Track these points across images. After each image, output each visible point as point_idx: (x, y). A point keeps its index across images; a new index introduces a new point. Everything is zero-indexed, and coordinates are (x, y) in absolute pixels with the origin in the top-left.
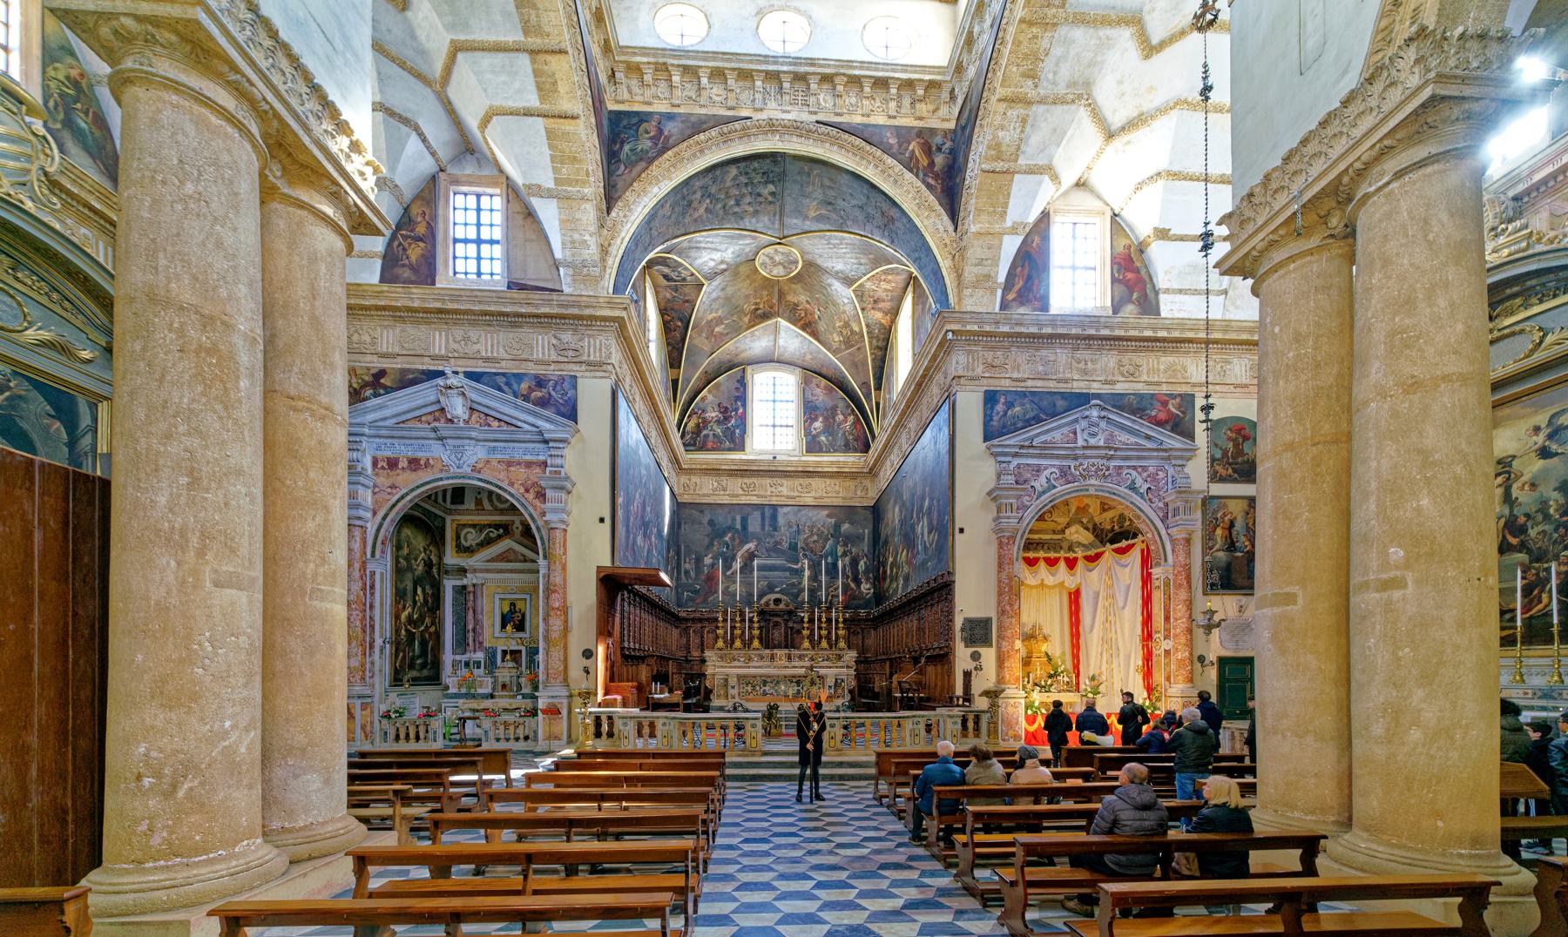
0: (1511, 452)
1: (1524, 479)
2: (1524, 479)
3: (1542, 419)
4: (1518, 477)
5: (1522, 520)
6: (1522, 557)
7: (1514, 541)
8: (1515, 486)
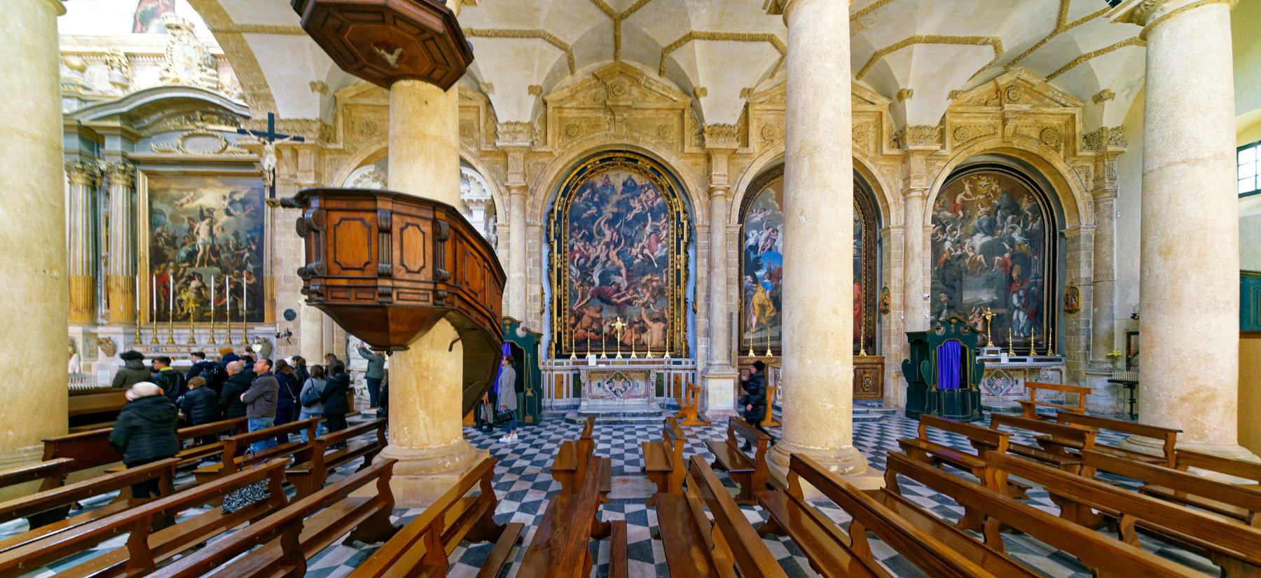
2: (219, 224)
3: (227, 192)
4: (215, 223)
5: (218, 248)
6: (217, 269)
7: (214, 259)
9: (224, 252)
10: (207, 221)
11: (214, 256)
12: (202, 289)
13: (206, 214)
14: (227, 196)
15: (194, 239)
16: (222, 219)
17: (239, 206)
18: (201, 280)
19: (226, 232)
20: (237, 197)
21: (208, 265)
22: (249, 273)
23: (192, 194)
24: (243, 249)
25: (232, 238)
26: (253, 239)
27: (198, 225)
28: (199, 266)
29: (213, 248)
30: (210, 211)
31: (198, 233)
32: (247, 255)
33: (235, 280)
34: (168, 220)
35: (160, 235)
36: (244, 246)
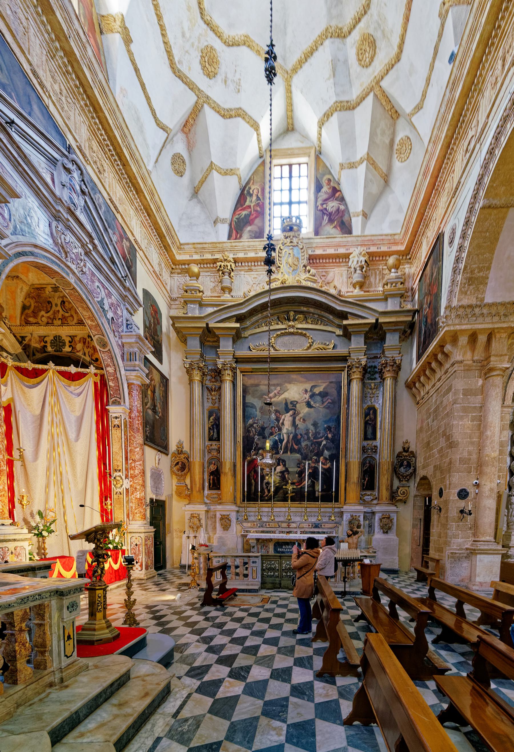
0: (296, 399)
1: (301, 415)
2: (301, 415)
3: (308, 386)
5: (299, 436)
7: (296, 447)
8: (297, 418)
9: (305, 440)
10: (291, 412)
11: (296, 445)
12: (285, 473)
13: (290, 406)
14: (309, 390)
15: (280, 429)
16: (304, 410)
17: (318, 398)
18: (284, 465)
19: (307, 422)
20: (317, 391)
21: (291, 453)
22: (325, 459)
23: (279, 388)
24: (322, 438)
25: (312, 428)
26: (329, 428)
27: (283, 417)
28: (283, 453)
29: (295, 436)
30: (294, 403)
31: (283, 424)
32: (324, 442)
33: (313, 465)
34: (258, 413)
35: (251, 426)
36: (321, 435)
